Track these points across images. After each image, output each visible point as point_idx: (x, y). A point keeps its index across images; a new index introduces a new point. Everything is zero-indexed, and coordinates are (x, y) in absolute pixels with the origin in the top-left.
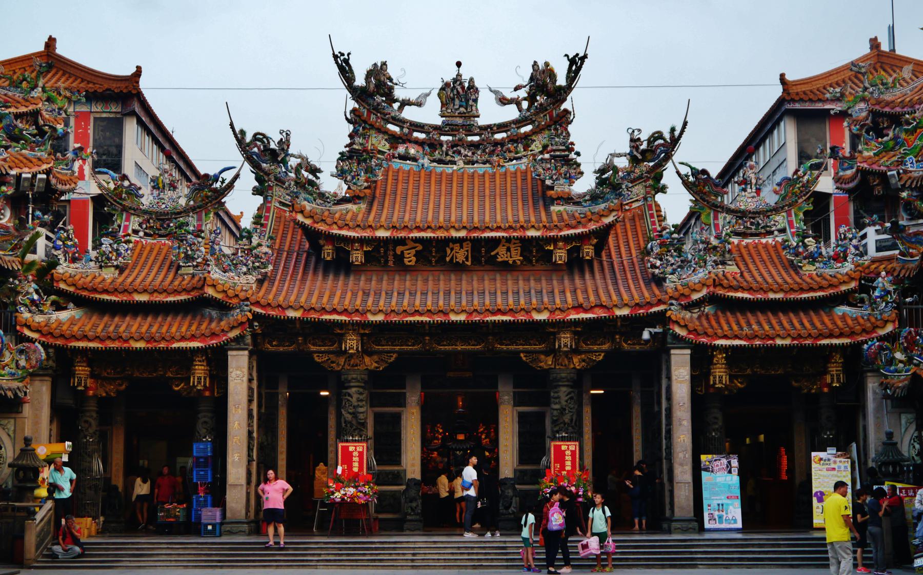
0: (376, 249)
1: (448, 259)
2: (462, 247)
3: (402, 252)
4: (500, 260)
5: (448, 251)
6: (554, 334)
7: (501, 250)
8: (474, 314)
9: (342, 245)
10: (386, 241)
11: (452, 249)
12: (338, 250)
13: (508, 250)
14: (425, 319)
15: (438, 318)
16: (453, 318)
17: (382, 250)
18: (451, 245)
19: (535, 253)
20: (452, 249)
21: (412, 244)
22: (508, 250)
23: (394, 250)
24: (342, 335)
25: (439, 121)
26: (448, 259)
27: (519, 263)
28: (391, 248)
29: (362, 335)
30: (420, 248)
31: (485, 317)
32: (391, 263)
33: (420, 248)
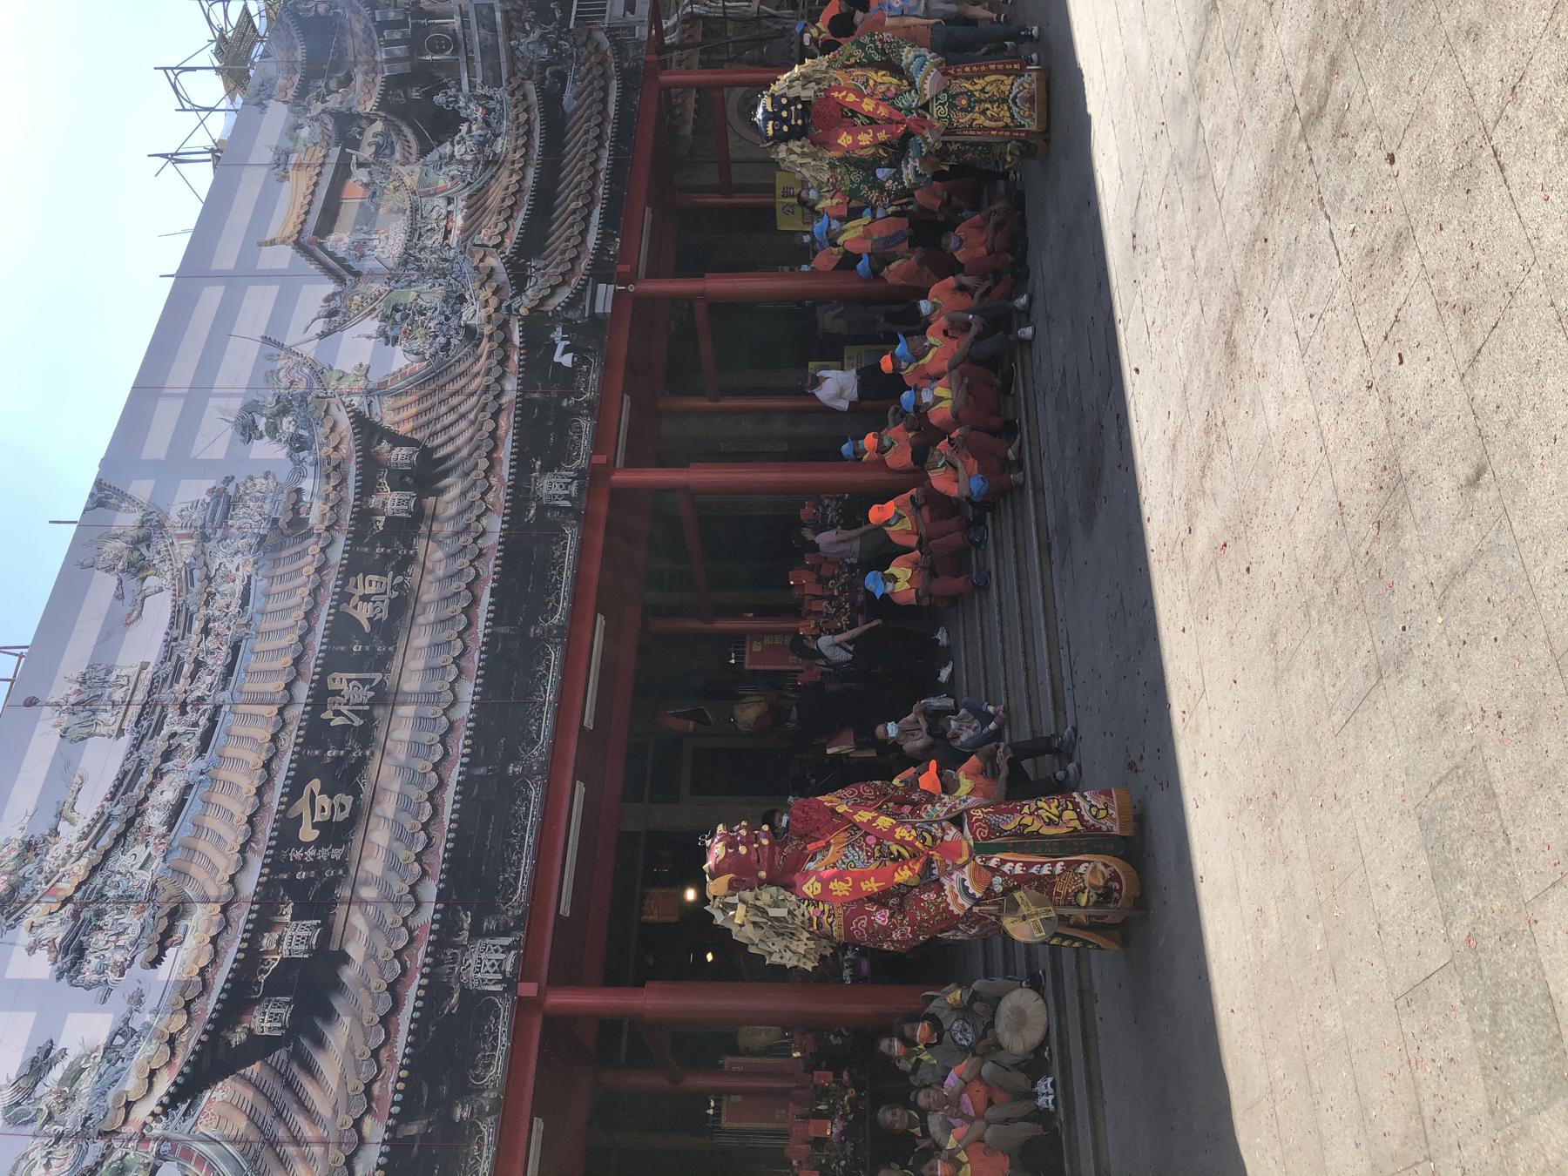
0: (296, 890)
1: (358, 722)
2: (338, 693)
3: (315, 826)
4: (384, 615)
5: (338, 721)
6: (542, 509)
7: (363, 613)
8: (463, 663)
9: (263, 978)
10: (275, 863)
11: (338, 713)
12: (277, 985)
13: (365, 598)
14: (454, 777)
15: (460, 745)
16: (464, 711)
17: (301, 875)
18: (323, 716)
19: (384, 546)
20: (338, 713)
21: (302, 805)
22: (365, 598)
23: (307, 845)
24: (465, 991)
25: (126, 740)
26: (358, 722)
27: (399, 579)
28: (298, 855)
29: (477, 932)
30: (316, 784)
31: (475, 640)
32: (337, 854)
33: (316, 784)
